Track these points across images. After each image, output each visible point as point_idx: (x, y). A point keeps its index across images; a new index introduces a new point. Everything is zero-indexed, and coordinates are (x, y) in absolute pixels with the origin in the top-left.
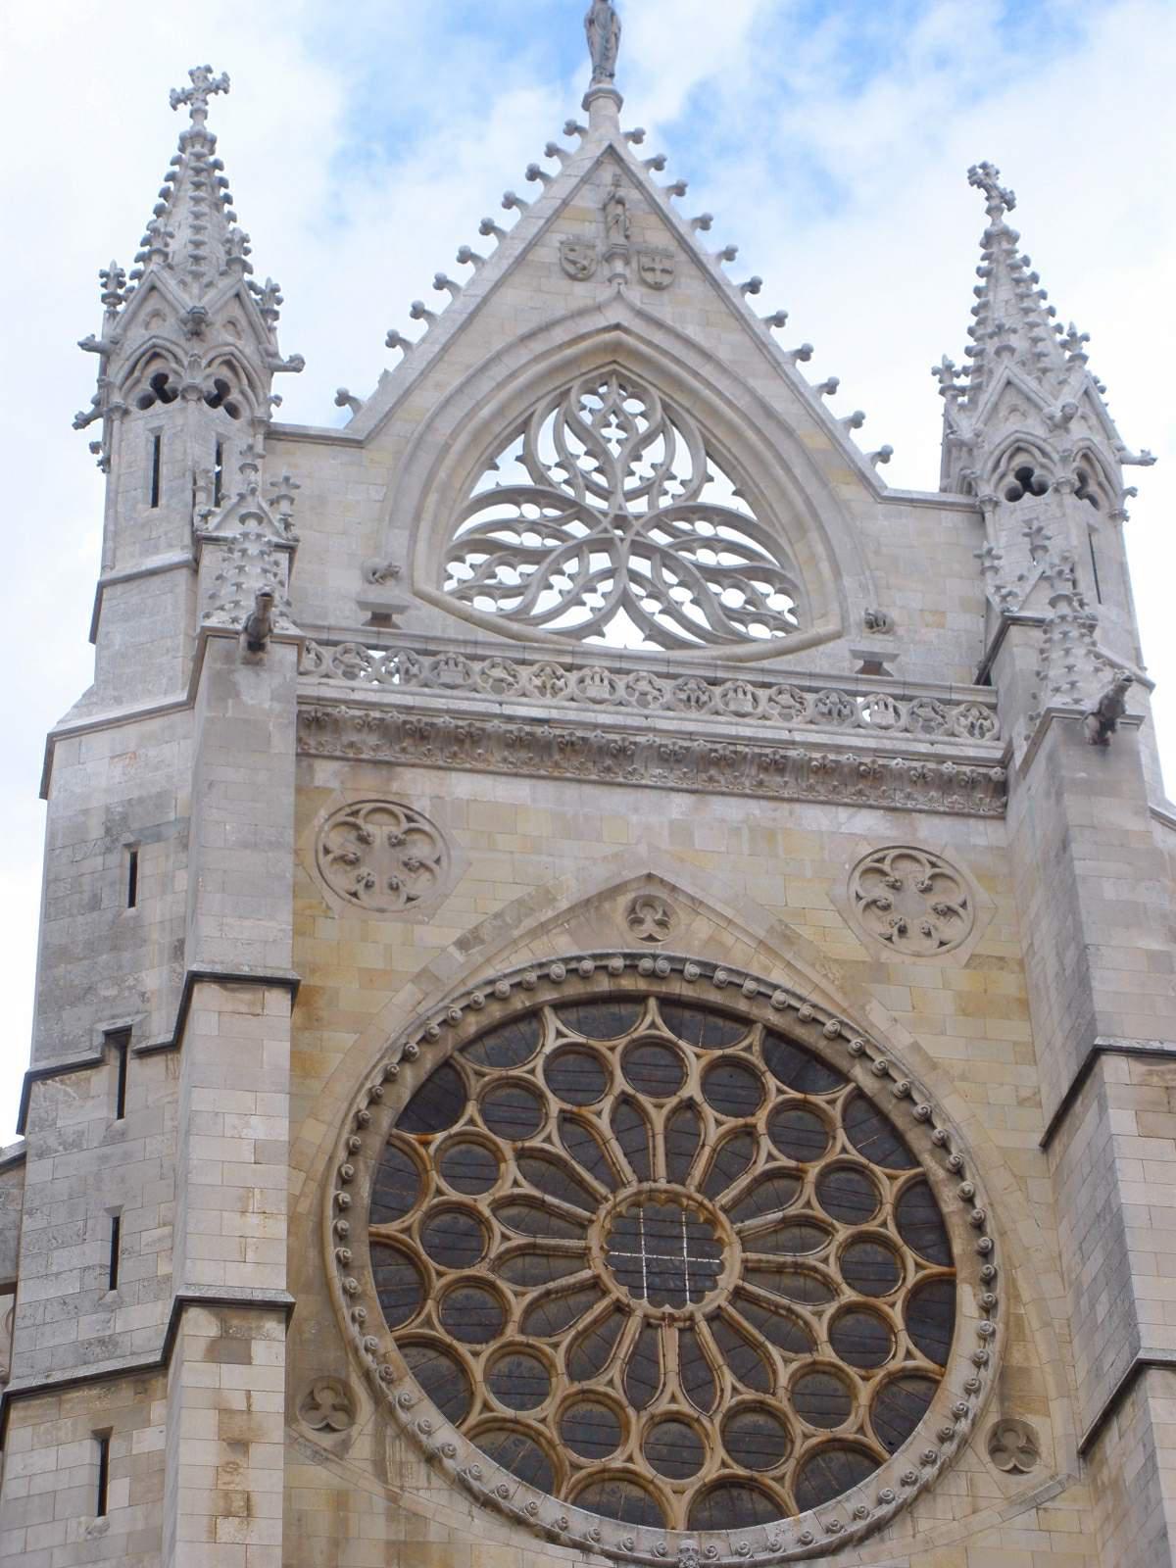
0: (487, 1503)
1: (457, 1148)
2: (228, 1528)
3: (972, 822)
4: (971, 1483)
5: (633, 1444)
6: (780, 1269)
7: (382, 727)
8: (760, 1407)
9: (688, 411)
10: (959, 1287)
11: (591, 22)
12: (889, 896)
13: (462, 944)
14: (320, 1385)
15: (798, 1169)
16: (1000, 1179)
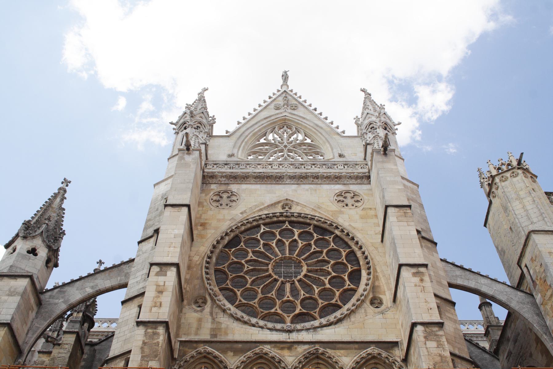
0: (238, 319)
1: (238, 252)
2: (154, 310)
3: (363, 185)
4: (365, 310)
5: (277, 307)
6: (317, 270)
7: (226, 177)
8: (311, 298)
9: (301, 128)
10: (362, 272)
11: (283, 76)
12: (344, 199)
13: (242, 213)
14: (198, 298)
15: (321, 251)
16: (371, 249)
